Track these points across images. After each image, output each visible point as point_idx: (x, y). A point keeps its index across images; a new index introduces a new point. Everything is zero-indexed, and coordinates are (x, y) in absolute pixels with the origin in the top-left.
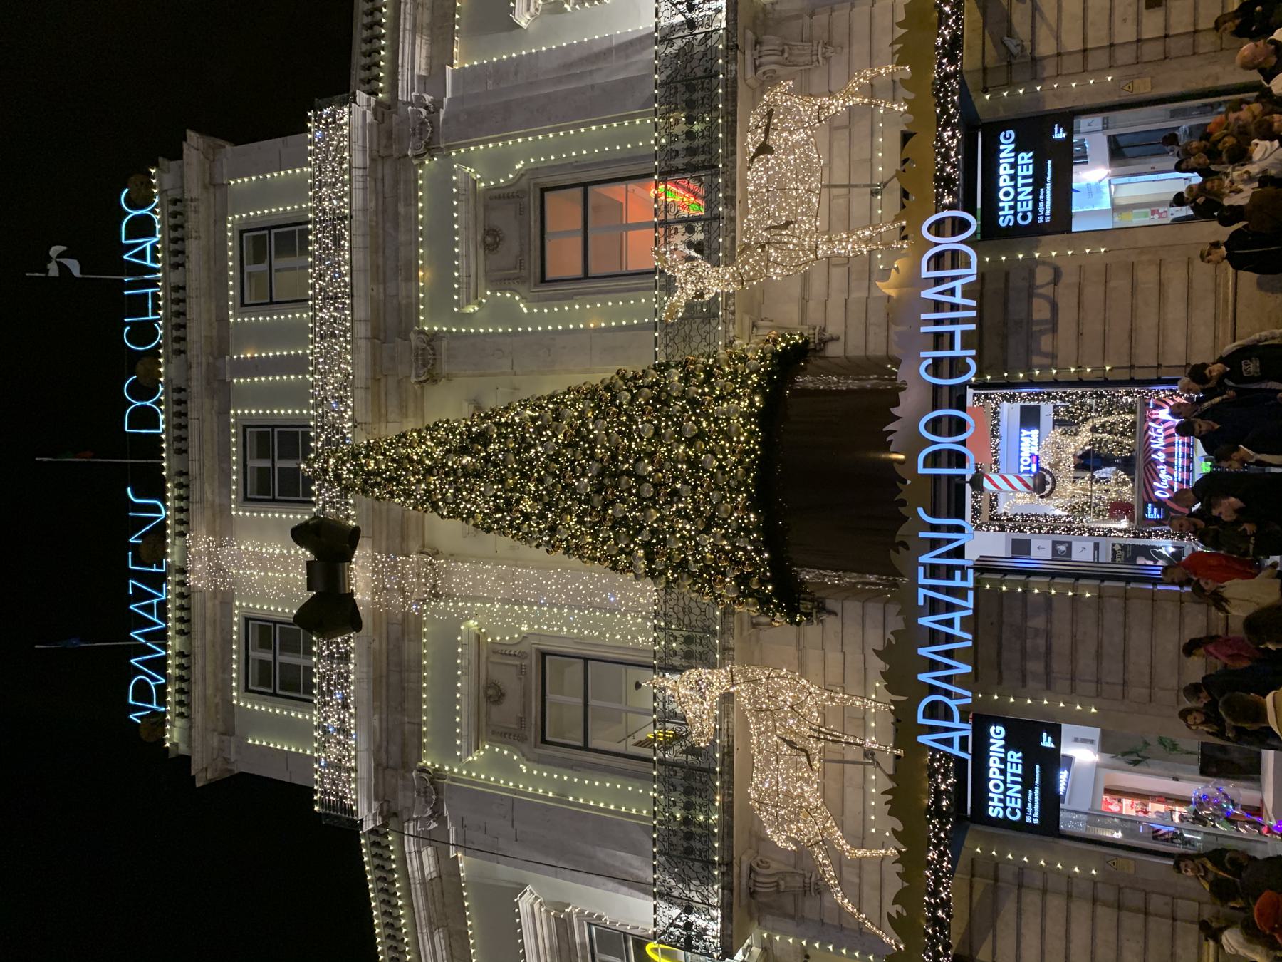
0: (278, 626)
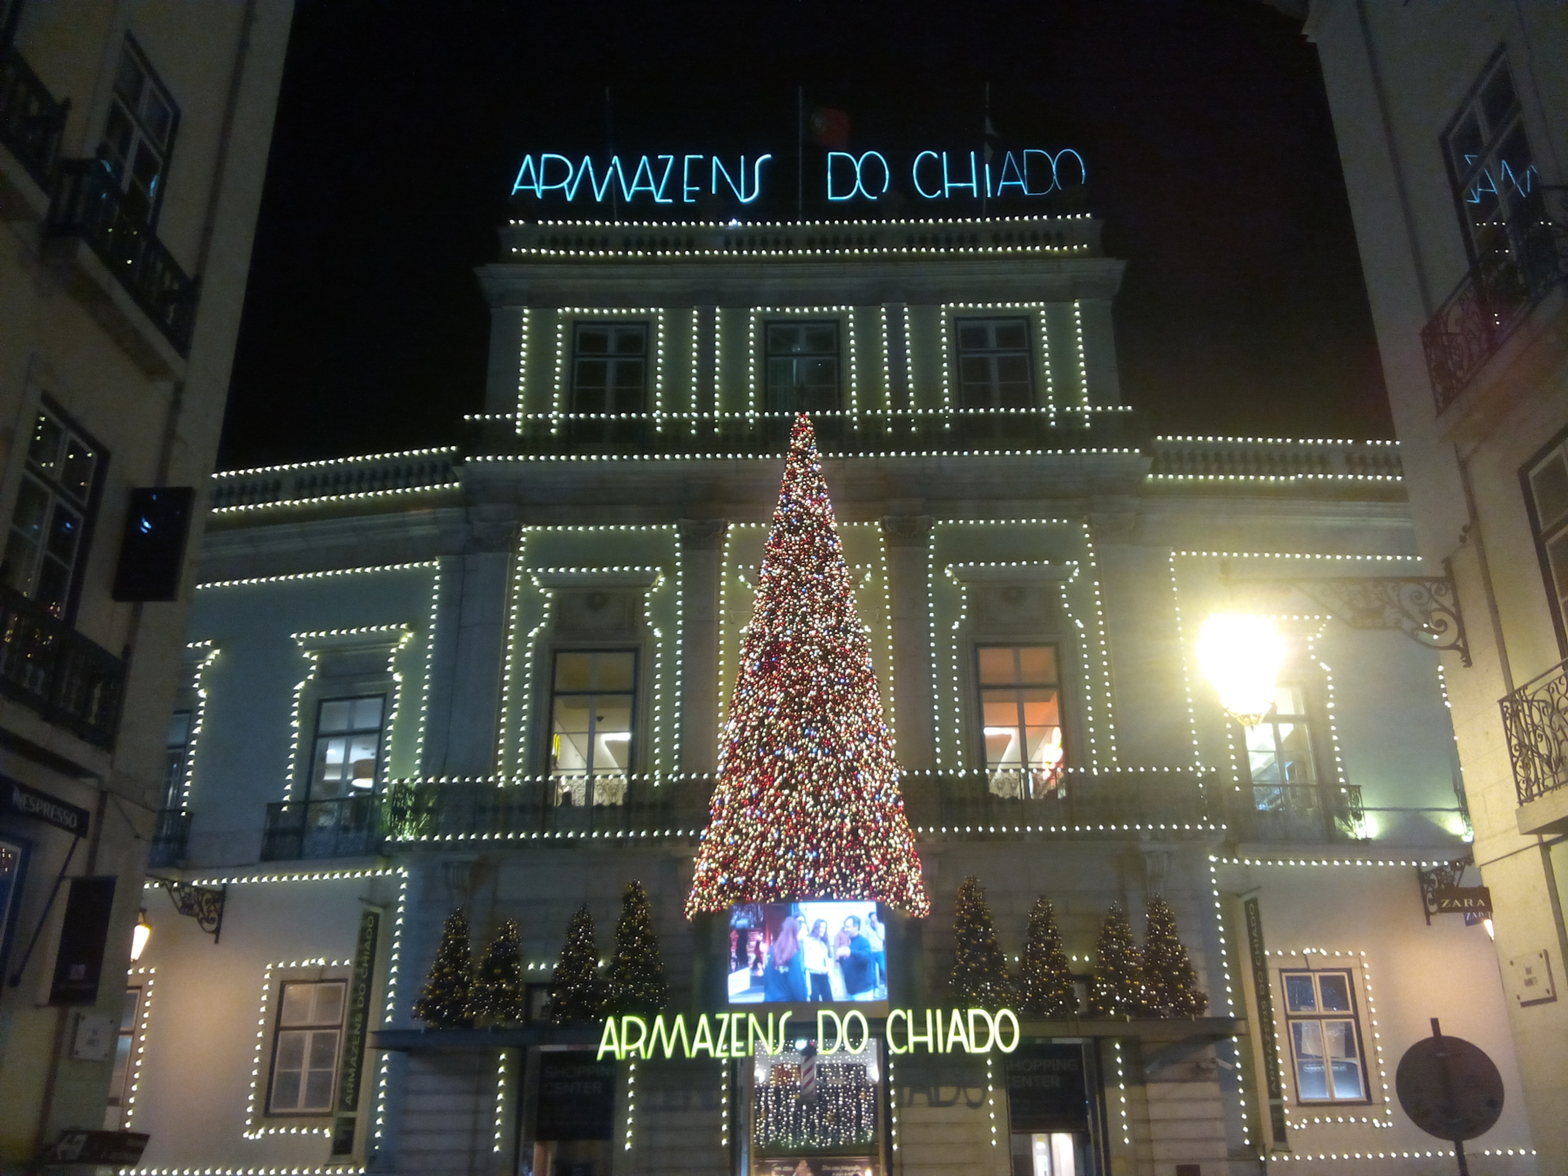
0: (642, 360)
